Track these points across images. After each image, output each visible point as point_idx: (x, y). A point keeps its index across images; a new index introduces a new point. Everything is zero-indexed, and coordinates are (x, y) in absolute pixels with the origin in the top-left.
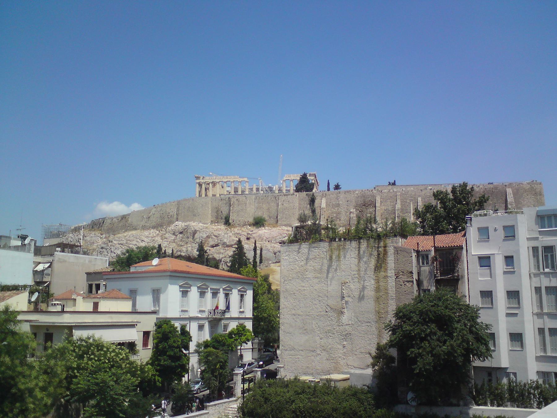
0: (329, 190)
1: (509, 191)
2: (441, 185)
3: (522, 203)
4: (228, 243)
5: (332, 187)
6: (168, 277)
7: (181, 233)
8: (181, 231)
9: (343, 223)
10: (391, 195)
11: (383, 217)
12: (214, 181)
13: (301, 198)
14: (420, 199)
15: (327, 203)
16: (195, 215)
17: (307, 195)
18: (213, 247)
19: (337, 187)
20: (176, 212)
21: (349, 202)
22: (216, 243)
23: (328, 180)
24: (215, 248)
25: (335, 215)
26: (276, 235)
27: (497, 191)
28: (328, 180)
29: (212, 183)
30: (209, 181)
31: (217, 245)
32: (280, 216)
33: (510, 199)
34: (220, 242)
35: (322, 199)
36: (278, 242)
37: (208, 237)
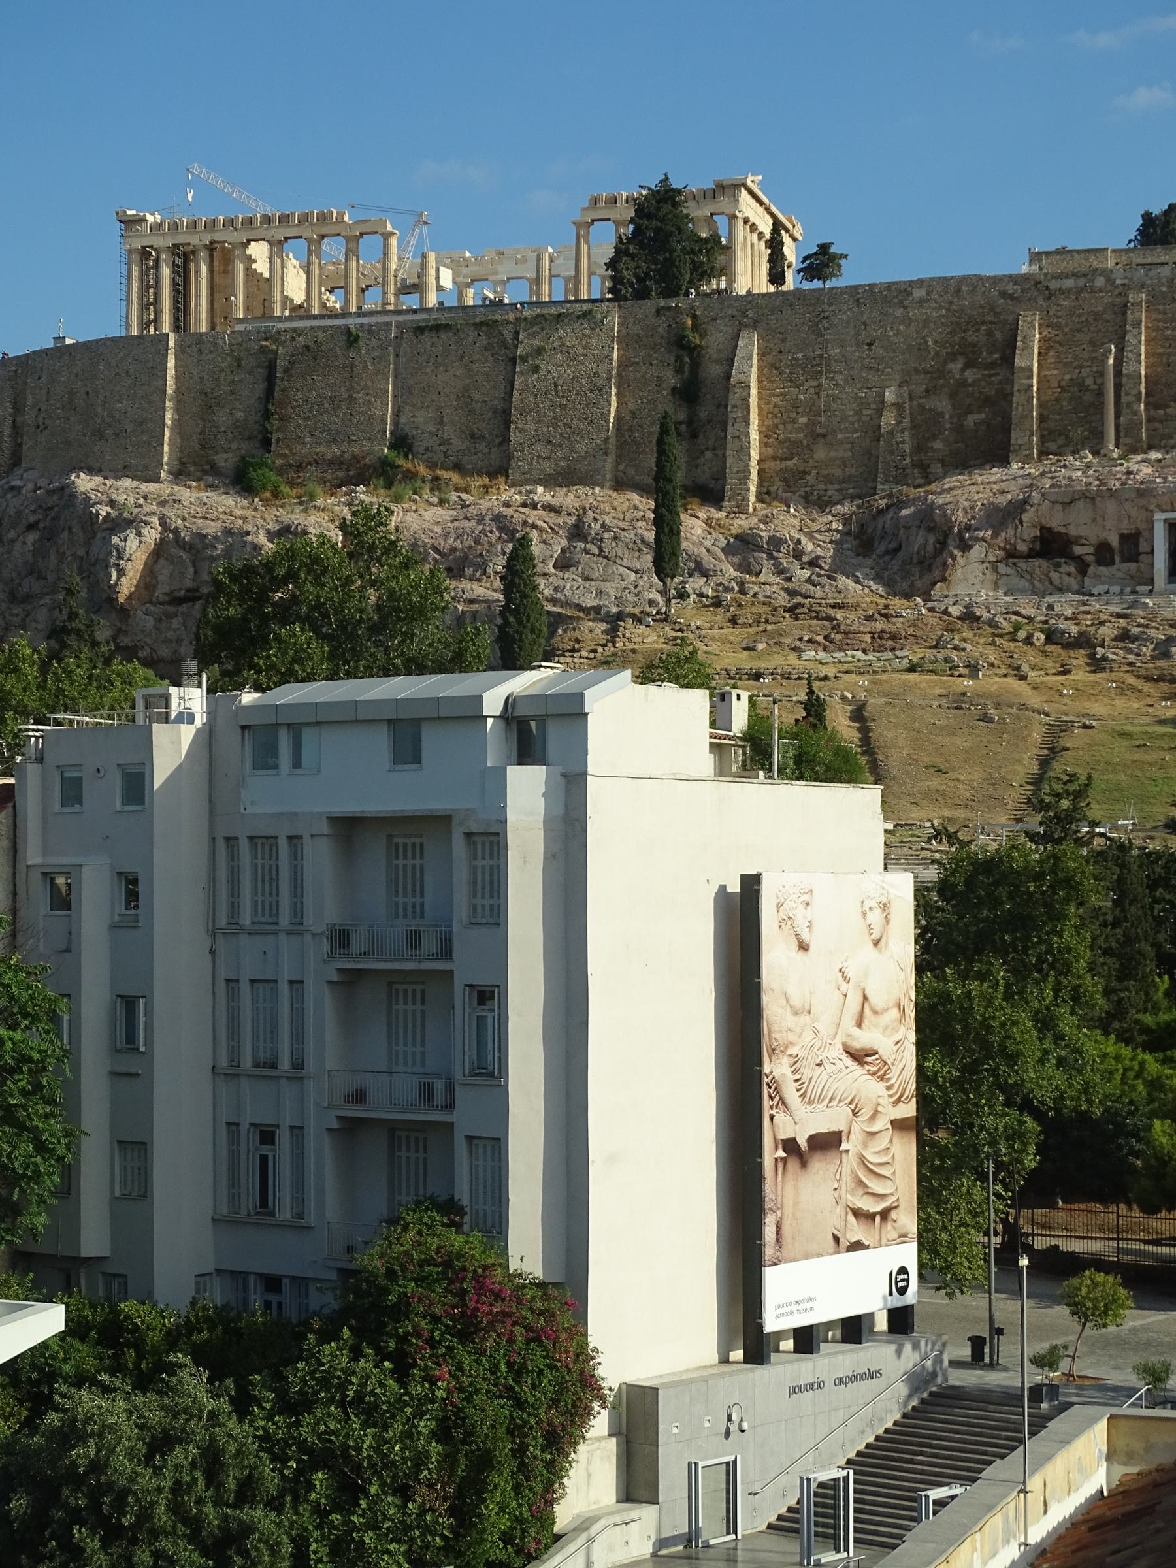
7: (31, 527)
8: (32, 519)
11: (1052, 425)
12: (218, 237)
13: (635, 329)
15: (762, 355)
16: (100, 435)
18: (177, 601)
20: (9, 422)
24: (184, 608)
25: (803, 420)
29: (211, 248)
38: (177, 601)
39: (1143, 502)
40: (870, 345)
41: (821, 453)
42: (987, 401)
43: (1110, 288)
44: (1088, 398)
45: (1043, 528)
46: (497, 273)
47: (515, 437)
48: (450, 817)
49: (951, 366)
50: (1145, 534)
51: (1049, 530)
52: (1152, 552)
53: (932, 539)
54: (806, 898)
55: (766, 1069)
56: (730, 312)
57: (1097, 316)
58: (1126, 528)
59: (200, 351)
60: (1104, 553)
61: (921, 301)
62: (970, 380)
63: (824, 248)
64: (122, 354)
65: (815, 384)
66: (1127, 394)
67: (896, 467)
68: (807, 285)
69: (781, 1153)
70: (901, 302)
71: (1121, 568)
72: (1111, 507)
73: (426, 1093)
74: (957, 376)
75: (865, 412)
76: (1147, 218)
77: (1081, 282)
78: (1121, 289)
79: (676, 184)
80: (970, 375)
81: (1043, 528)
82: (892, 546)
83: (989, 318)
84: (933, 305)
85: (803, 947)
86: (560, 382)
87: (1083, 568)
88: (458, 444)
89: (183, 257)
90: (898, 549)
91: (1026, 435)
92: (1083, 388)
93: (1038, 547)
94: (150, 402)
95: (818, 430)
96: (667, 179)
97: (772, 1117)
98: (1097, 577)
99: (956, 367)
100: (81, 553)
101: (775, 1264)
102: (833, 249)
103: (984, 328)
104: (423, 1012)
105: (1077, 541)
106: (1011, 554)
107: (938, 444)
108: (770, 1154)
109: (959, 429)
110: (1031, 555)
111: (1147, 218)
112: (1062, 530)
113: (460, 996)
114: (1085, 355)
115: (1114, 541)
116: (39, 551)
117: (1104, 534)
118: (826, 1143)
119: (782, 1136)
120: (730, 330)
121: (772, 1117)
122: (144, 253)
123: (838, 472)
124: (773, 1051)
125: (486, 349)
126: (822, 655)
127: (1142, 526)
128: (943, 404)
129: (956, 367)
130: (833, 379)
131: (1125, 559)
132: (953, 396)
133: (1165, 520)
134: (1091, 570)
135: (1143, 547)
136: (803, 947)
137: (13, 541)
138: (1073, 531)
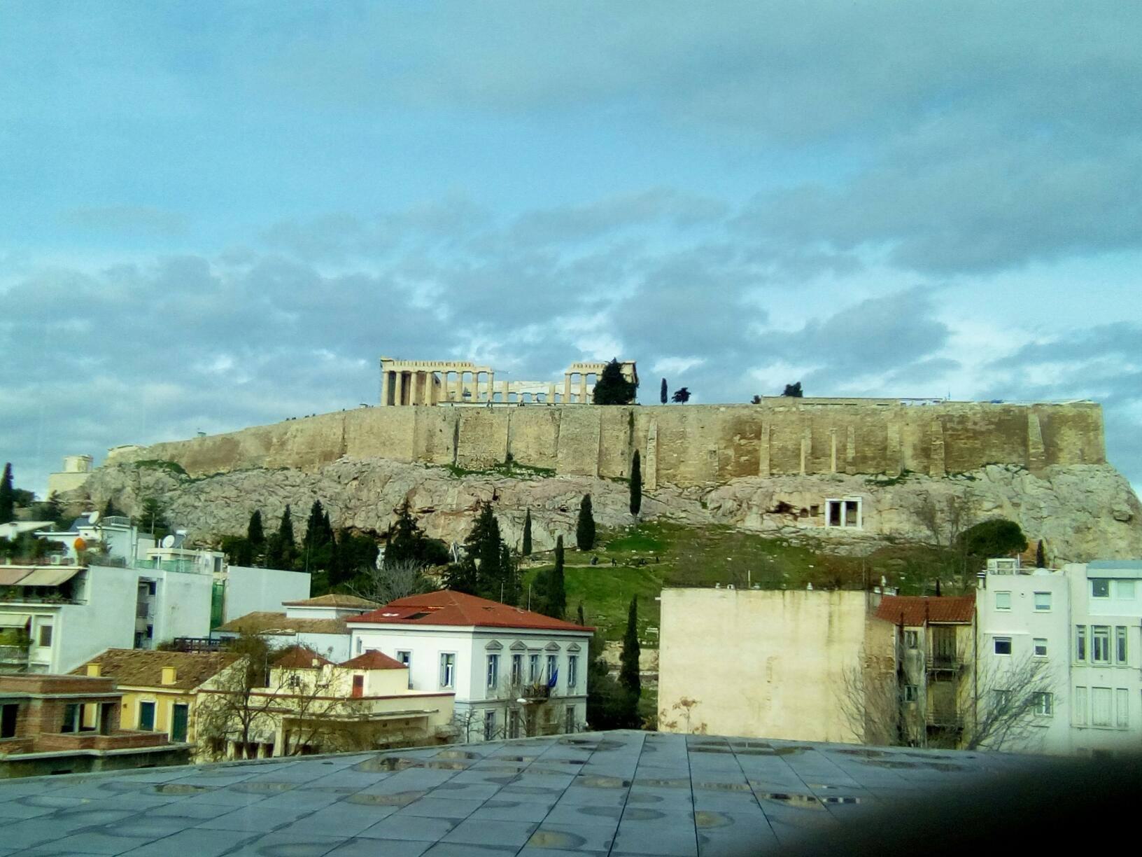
0: (664, 400)
1: (1034, 419)
3: (1057, 444)
4: (454, 506)
5: (671, 394)
6: (471, 635)
7: (355, 479)
8: (356, 476)
9: (691, 473)
11: (775, 463)
14: (851, 429)
19: (683, 395)
21: (705, 430)
22: (430, 505)
23: (664, 381)
24: (427, 515)
25: (675, 455)
26: (553, 494)
27: (1009, 418)
28: (664, 381)
31: (430, 511)
33: (1034, 434)
34: (437, 503)
36: (559, 508)
37: (413, 492)
38: (424, 512)
39: (821, 494)
41: (682, 468)
42: (749, 452)
47: (560, 455)
49: (735, 438)
50: (821, 506)
52: (824, 513)
53: (735, 504)
56: (647, 412)
57: (793, 422)
58: (814, 503)
59: (428, 414)
60: (804, 511)
61: (723, 412)
63: (684, 390)
68: (675, 403)
71: (810, 518)
72: (808, 495)
77: (787, 409)
79: (619, 361)
80: (743, 442)
82: (717, 505)
87: (796, 517)
88: (535, 456)
89: (406, 376)
90: (720, 507)
91: (764, 466)
92: (787, 449)
95: (682, 459)
98: (801, 522)
99: (738, 437)
100: (379, 490)
102: (687, 391)
106: (768, 512)
107: (729, 468)
109: (738, 462)
110: (776, 512)
115: (808, 508)
116: (358, 489)
122: (392, 374)
123: (689, 476)
127: (820, 503)
128: (731, 452)
129: (738, 437)
131: (813, 516)
132: (735, 450)
133: (830, 502)
134: (799, 519)
135: (820, 511)
137: (346, 484)
138: (792, 504)
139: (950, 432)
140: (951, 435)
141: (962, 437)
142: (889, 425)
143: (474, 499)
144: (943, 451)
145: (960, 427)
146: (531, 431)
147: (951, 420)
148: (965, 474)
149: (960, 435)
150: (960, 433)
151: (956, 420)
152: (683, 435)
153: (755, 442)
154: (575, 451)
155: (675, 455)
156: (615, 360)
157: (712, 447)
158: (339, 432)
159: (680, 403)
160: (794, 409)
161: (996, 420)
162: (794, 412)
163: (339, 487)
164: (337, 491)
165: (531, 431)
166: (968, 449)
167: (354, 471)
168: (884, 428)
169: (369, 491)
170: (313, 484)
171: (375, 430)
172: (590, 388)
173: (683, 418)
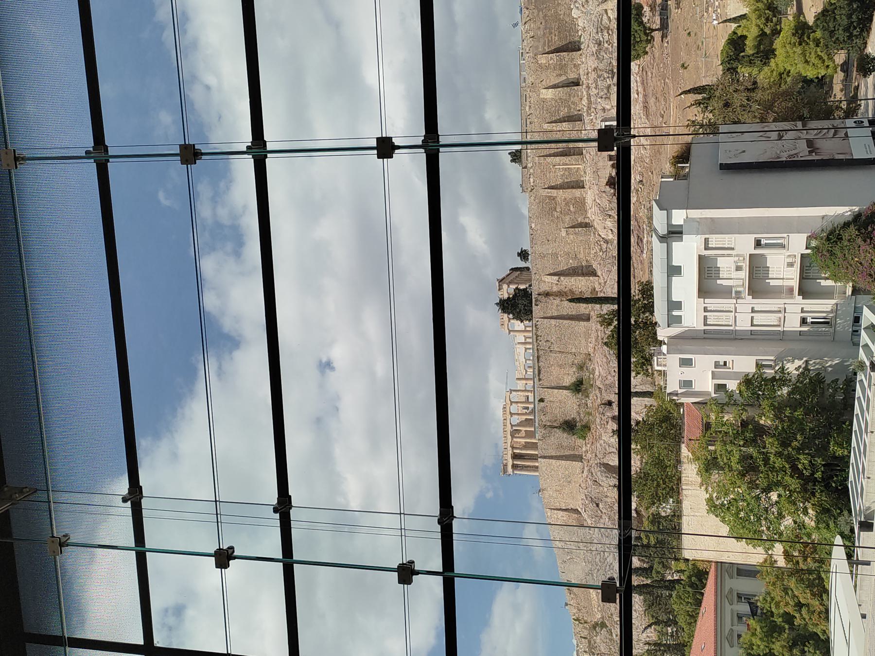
2: (521, 87)
5: (522, 264)
7: (598, 505)
8: (595, 505)
10: (539, 170)
17: (537, 305)
19: (524, 255)
21: (550, 238)
25: (571, 261)
29: (513, 448)
30: (511, 452)
32: (572, 348)
35: (545, 282)
40: (548, 241)
41: (582, 256)
43: (533, 168)
44: (567, 173)
45: (607, 185)
46: (523, 362)
47: (573, 350)
48: (699, 255)
51: (607, 182)
54: (728, 152)
55: (784, 159)
62: (560, 210)
63: (519, 255)
64: (545, 474)
65: (560, 257)
66: (566, 161)
67: (586, 232)
68: (530, 260)
69: (814, 154)
70: (536, 231)
72: (601, 164)
73: (791, 265)
74: (559, 214)
75: (569, 242)
76: (512, 161)
78: (534, 164)
81: (607, 185)
83: (541, 204)
84: (537, 221)
85: (744, 152)
86: (557, 337)
89: (515, 457)
90: (611, 230)
93: (612, 186)
94: (559, 466)
96: (497, 304)
97: (801, 157)
99: (556, 214)
101: (852, 155)
102: (520, 252)
103: (544, 206)
104: (763, 267)
105: (610, 174)
108: (814, 157)
111: (513, 161)
112: (607, 179)
113: (759, 251)
114: (553, 174)
117: (609, 165)
118: (810, 143)
119: (808, 154)
120: (543, 284)
121: (801, 157)
122: (515, 467)
124: (779, 158)
125: (546, 359)
126: (645, 252)
128: (567, 218)
129: (556, 214)
130: (558, 252)
136: (744, 152)
138: (608, 175)
139: (546, 48)
140: (549, 47)
141: (550, 39)
142: (542, 96)
143: (610, 422)
144: (562, 54)
145: (542, 41)
146: (555, 371)
147: (537, 48)
148: (580, 34)
149: (548, 40)
150: (547, 40)
151: (536, 44)
152: (555, 255)
153: (558, 199)
154: (569, 338)
155: (571, 261)
156: (497, 304)
157: (564, 234)
158: (561, 513)
159: (529, 257)
160: (531, 171)
161: (536, 11)
162: (534, 170)
163: (604, 516)
164: (607, 520)
165: (555, 371)
166: (559, 32)
167: (592, 506)
168: (544, 101)
169: (606, 497)
170: (602, 535)
171: (559, 488)
172: (518, 325)
173: (543, 256)
